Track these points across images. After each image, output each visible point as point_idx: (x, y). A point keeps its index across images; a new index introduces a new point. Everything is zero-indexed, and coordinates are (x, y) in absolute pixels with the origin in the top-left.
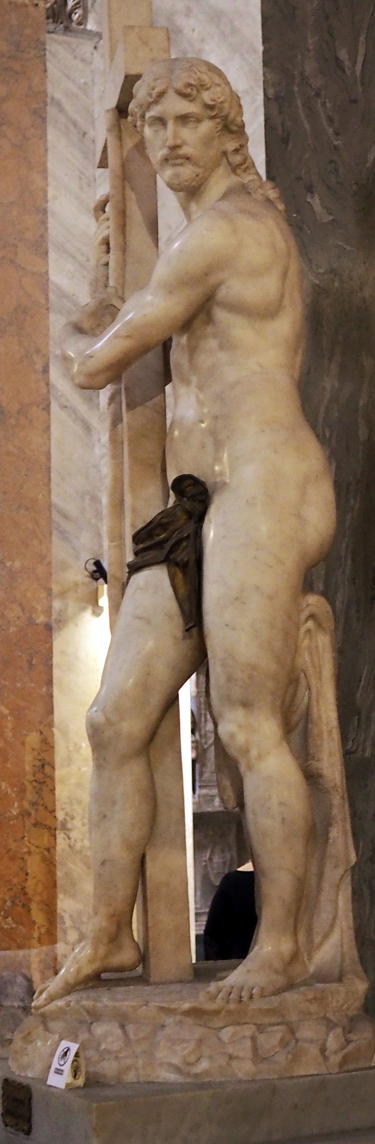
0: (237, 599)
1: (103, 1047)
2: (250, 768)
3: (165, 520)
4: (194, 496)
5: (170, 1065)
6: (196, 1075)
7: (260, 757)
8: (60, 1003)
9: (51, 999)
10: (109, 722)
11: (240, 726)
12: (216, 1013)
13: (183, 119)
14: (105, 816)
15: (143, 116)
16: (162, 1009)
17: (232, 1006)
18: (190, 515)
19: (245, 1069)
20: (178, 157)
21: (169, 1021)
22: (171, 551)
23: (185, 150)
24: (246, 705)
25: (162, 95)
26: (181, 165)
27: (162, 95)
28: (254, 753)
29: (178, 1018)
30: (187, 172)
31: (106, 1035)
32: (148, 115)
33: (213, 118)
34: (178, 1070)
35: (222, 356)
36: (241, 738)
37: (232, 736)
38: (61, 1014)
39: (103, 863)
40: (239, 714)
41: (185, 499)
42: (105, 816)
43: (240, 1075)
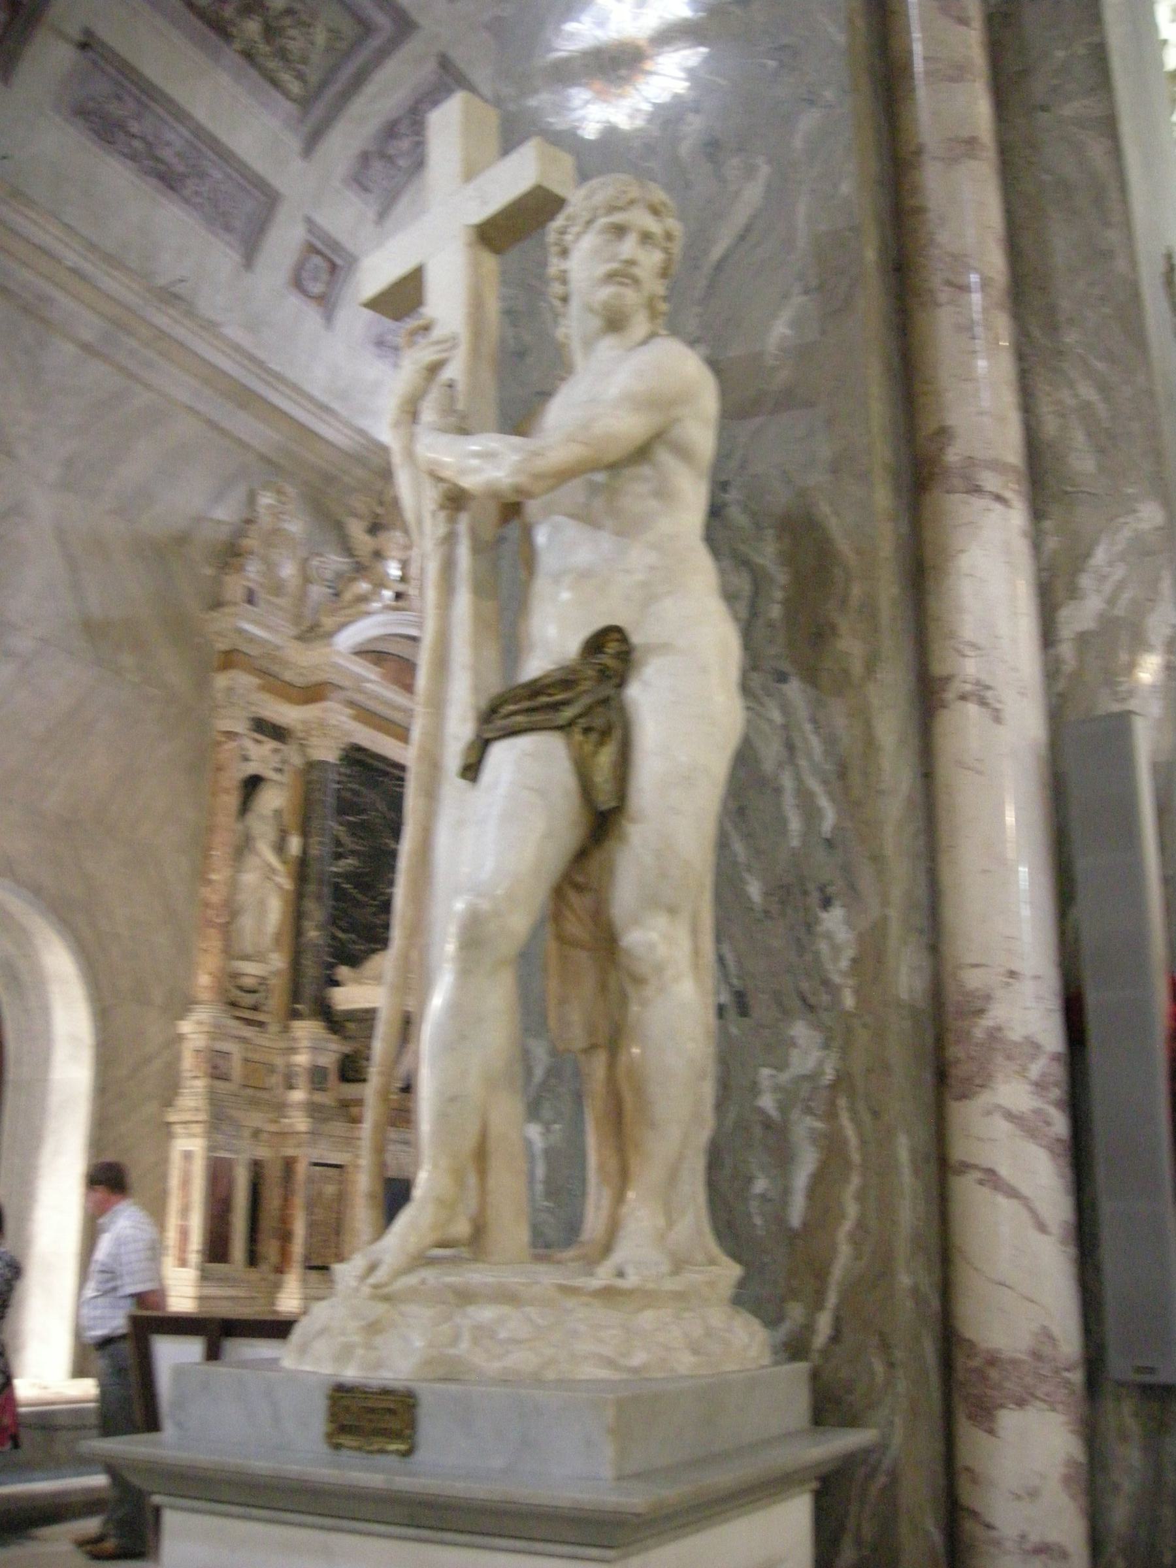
3: (570, 677)
4: (610, 654)
6: (635, 1370)
8: (412, 1280)
13: (646, 238)
15: (589, 223)
17: (650, 1286)
18: (604, 674)
19: (685, 1362)
20: (626, 276)
21: (571, 1303)
22: (586, 713)
23: (636, 271)
24: (672, 911)
25: (632, 202)
26: (626, 285)
27: (632, 202)
29: (585, 1299)
30: (631, 296)
33: (666, 250)
34: (610, 1363)
35: (653, 504)
36: (662, 951)
39: (453, 1099)
43: (683, 1370)
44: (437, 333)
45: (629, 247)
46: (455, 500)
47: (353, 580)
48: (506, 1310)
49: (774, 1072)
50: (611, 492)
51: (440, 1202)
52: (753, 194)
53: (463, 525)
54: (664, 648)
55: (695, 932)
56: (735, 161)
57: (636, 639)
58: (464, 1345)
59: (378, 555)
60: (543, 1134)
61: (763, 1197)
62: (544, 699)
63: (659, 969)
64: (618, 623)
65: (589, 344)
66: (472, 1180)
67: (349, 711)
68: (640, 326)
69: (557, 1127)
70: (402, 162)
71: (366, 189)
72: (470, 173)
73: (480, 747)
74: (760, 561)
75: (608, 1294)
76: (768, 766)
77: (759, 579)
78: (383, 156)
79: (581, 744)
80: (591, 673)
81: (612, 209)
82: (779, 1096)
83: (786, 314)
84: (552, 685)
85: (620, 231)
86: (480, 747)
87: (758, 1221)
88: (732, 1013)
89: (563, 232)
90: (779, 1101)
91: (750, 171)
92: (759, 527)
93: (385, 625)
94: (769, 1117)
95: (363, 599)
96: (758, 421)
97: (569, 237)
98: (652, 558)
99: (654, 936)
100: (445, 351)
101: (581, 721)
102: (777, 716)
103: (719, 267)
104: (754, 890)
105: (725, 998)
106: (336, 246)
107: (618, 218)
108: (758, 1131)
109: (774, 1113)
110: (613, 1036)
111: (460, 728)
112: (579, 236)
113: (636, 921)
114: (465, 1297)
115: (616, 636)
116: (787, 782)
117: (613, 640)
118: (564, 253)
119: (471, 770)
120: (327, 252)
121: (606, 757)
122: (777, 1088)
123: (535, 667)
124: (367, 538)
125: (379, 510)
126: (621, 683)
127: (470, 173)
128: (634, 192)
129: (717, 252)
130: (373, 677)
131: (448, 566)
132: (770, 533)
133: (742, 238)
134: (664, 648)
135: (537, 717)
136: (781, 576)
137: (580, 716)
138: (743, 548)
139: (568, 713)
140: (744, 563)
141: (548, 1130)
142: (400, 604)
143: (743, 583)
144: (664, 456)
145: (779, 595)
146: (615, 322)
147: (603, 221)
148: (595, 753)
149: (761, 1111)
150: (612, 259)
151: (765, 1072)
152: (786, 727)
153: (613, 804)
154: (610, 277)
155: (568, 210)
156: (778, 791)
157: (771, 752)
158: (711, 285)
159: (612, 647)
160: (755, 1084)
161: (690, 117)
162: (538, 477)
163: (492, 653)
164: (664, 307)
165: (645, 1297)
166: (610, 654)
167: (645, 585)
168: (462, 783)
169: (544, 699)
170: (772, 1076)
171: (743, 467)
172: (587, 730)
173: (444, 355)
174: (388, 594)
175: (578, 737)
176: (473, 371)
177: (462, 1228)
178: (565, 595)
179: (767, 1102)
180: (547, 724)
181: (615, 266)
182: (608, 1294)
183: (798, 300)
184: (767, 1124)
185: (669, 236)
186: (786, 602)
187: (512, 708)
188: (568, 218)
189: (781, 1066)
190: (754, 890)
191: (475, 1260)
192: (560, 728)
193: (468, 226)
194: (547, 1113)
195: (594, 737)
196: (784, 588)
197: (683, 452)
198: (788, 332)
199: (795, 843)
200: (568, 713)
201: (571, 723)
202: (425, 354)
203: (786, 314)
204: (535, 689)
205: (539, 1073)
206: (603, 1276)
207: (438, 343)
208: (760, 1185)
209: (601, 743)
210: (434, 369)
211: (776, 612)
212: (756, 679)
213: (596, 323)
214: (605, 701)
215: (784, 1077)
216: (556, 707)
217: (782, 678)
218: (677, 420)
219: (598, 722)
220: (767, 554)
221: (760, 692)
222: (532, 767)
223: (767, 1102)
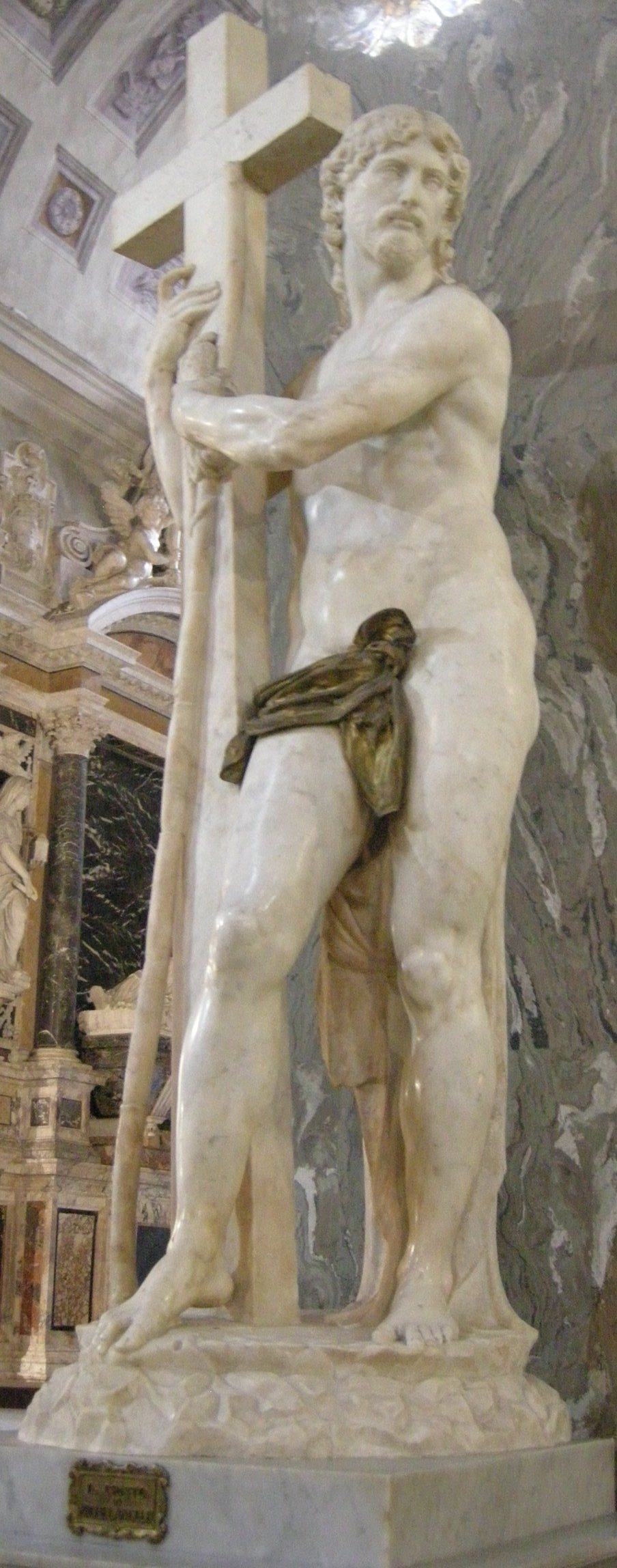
0: (474, 779)
1: (266, 1406)
2: (446, 1018)
3: (346, 667)
4: (389, 641)
5: (374, 1431)
7: (463, 1005)
8: (166, 1343)
9: (148, 1337)
10: (261, 931)
11: (447, 957)
12: (412, 1359)
13: (429, 175)
14: (225, 1070)
16: (332, 1353)
17: (434, 1351)
18: (382, 662)
21: (342, 1371)
23: (418, 213)
24: (459, 929)
25: (413, 137)
27: (413, 137)
28: (456, 998)
29: (359, 1366)
30: (412, 240)
31: (265, 1390)
32: (380, 158)
33: (451, 189)
35: (438, 473)
36: (447, 974)
37: (435, 970)
38: (165, 1361)
39: (212, 1141)
40: (447, 940)
41: (381, 643)
42: (225, 1070)
44: (196, 283)
45: (410, 186)
46: (217, 469)
47: (107, 553)
48: (271, 1377)
49: (576, 1110)
50: (391, 460)
51: (197, 1256)
52: (551, 123)
53: (226, 499)
54: (450, 633)
55: (483, 953)
56: (531, 88)
57: (418, 624)
58: (224, 1416)
59: (136, 523)
60: (315, 1179)
61: (563, 1251)
62: (314, 692)
63: (445, 994)
64: (399, 606)
65: (366, 296)
66: (234, 1230)
67: (105, 700)
68: (424, 274)
69: (330, 1171)
70: (164, 86)
71: (125, 116)
72: (234, 105)
73: (244, 746)
74: (560, 535)
75: (385, 1361)
76: (569, 766)
77: (557, 555)
78: (142, 76)
79: (356, 743)
80: (367, 661)
81: (390, 145)
82: (581, 1137)
83: (588, 259)
84: (324, 675)
85: (400, 169)
86: (244, 746)
87: (557, 1278)
88: (527, 1042)
89: (336, 171)
90: (578, 1143)
91: (547, 99)
92: (555, 495)
93: (144, 602)
94: (568, 1160)
95: (119, 573)
96: (559, 377)
97: (344, 176)
98: (437, 532)
99: (438, 957)
100: (206, 302)
101: (355, 715)
102: (578, 710)
103: (513, 206)
104: (553, 904)
105: (518, 1026)
106: (92, 179)
107: (398, 154)
108: (556, 1177)
109: (575, 1157)
110: (392, 1070)
111: (222, 725)
112: (354, 176)
113: (419, 940)
114: (224, 1363)
115: (398, 620)
116: (591, 786)
117: (394, 625)
118: (339, 193)
119: (235, 771)
120: (80, 184)
121: (385, 756)
122: (578, 1128)
123: (306, 654)
124: (124, 504)
125: (139, 474)
126: (402, 675)
127: (234, 105)
128: (416, 125)
129: (510, 191)
130: (133, 661)
131: (210, 542)
132: (571, 505)
133: (538, 173)
134: (450, 633)
135: (308, 712)
136: (583, 552)
137: (356, 709)
138: (539, 521)
140: (539, 536)
141: (320, 1173)
142: (158, 579)
143: (540, 560)
144: (450, 420)
145: (579, 573)
146: (394, 270)
147: (380, 158)
148: (373, 754)
149: (560, 1152)
150: (395, 199)
151: (565, 1110)
152: (587, 720)
153: (392, 809)
154: (390, 219)
155: (342, 145)
156: (580, 793)
157: (570, 750)
158: (504, 224)
159: (391, 634)
160: (554, 1122)
161: (480, 38)
162: (307, 444)
163: (257, 639)
164: (451, 252)
165: (427, 1365)
166: (389, 641)
167: (428, 563)
168: (225, 785)
169: (314, 692)
170: (572, 1114)
171: (539, 430)
172: (362, 727)
173: (207, 307)
174: (148, 568)
175: (354, 734)
176: (237, 325)
177: (222, 1285)
178: (340, 575)
179: (567, 1144)
180: (317, 720)
181: (395, 207)
182: (385, 1361)
183: (599, 242)
184: (567, 1169)
185: (455, 174)
186: (587, 581)
187: (282, 701)
188: (343, 155)
189: (584, 1103)
190: (553, 904)
191: (238, 1320)
192: (335, 724)
194: (319, 1156)
195: (371, 733)
196: (585, 565)
197: (472, 415)
198: (591, 279)
199: (598, 852)
200: (344, 706)
201: (346, 718)
202: (184, 305)
203: (588, 259)
204: (307, 679)
205: (311, 1110)
206: (381, 1339)
207: (201, 293)
208: (559, 1237)
209: (378, 741)
210: (194, 322)
211: (577, 591)
212: (555, 669)
213: (374, 271)
214: (384, 694)
215: (587, 1116)
216: (329, 700)
217: (583, 666)
218: (463, 379)
219: (377, 718)
220: (567, 527)
221: (560, 684)
222: (301, 769)
223: (567, 1144)
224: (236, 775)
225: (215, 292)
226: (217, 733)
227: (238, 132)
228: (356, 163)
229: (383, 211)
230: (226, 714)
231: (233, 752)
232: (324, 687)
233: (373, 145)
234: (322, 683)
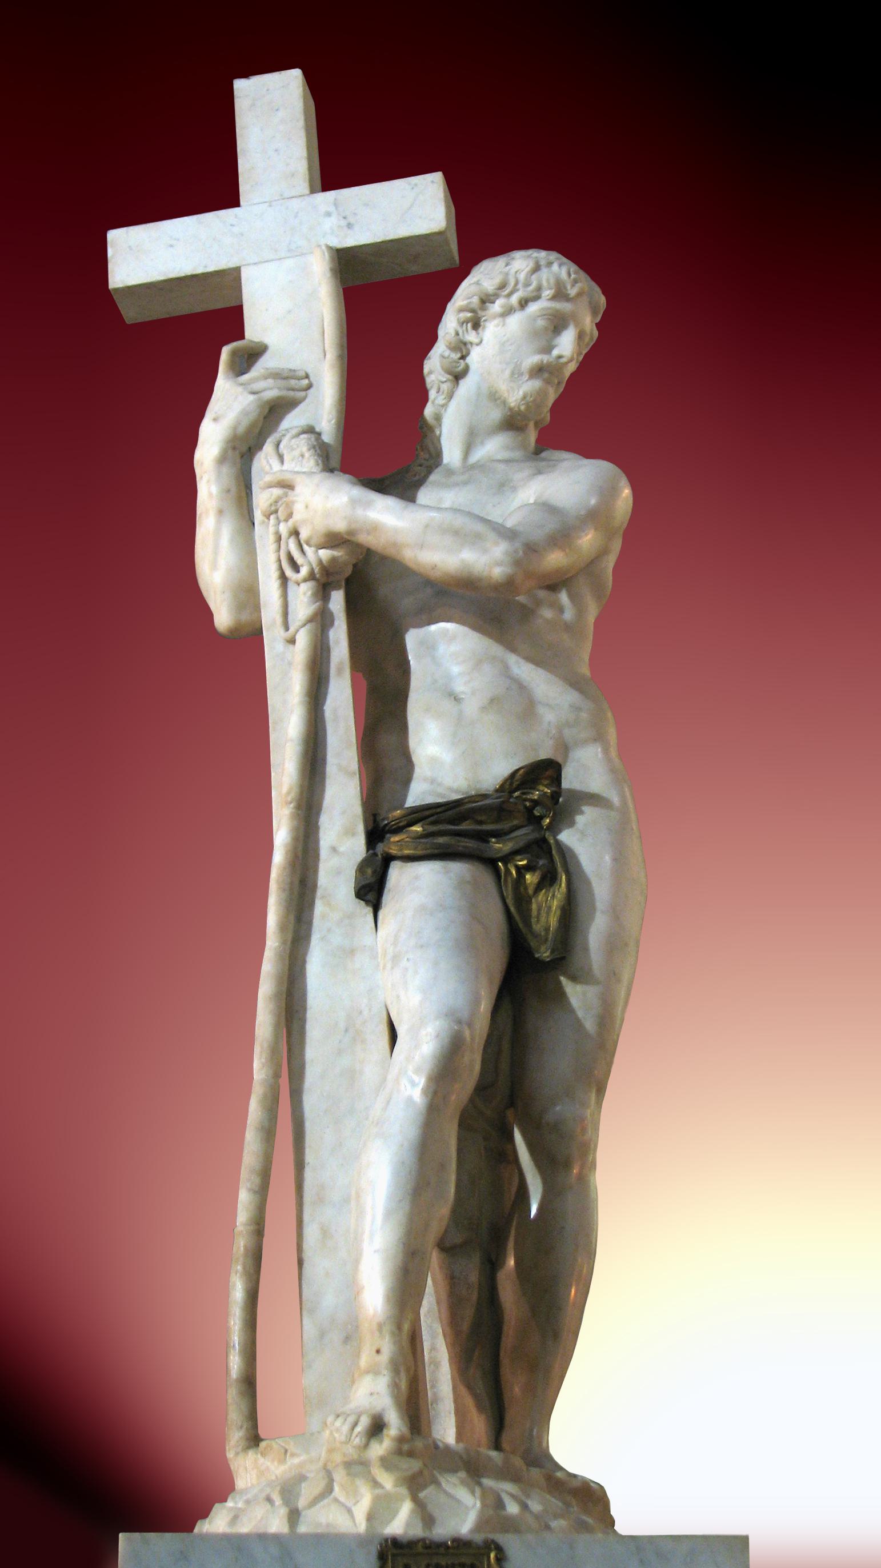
119: (371, 890)
135: (470, 844)
139: (498, 847)
169: (465, 826)
192: (491, 863)
193: (330, 248)
213: (496, 415)
224: (371, 896)
225: (306, 382)
226: (334, 849)
227: (328, 214)
228: (514, 299)
229: (535, 359)
230: (349, 832)
231: (369, 871)
232: (481, 823)
233: (539, 289)
234: (479, 818)
